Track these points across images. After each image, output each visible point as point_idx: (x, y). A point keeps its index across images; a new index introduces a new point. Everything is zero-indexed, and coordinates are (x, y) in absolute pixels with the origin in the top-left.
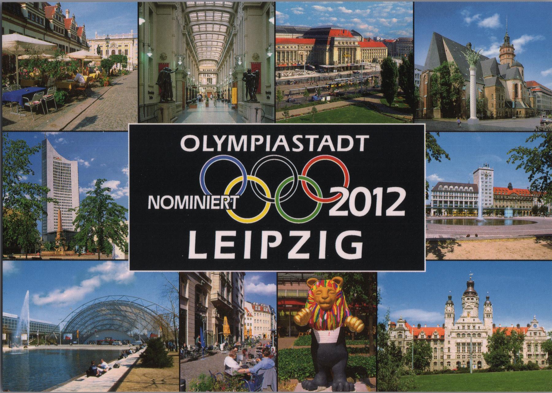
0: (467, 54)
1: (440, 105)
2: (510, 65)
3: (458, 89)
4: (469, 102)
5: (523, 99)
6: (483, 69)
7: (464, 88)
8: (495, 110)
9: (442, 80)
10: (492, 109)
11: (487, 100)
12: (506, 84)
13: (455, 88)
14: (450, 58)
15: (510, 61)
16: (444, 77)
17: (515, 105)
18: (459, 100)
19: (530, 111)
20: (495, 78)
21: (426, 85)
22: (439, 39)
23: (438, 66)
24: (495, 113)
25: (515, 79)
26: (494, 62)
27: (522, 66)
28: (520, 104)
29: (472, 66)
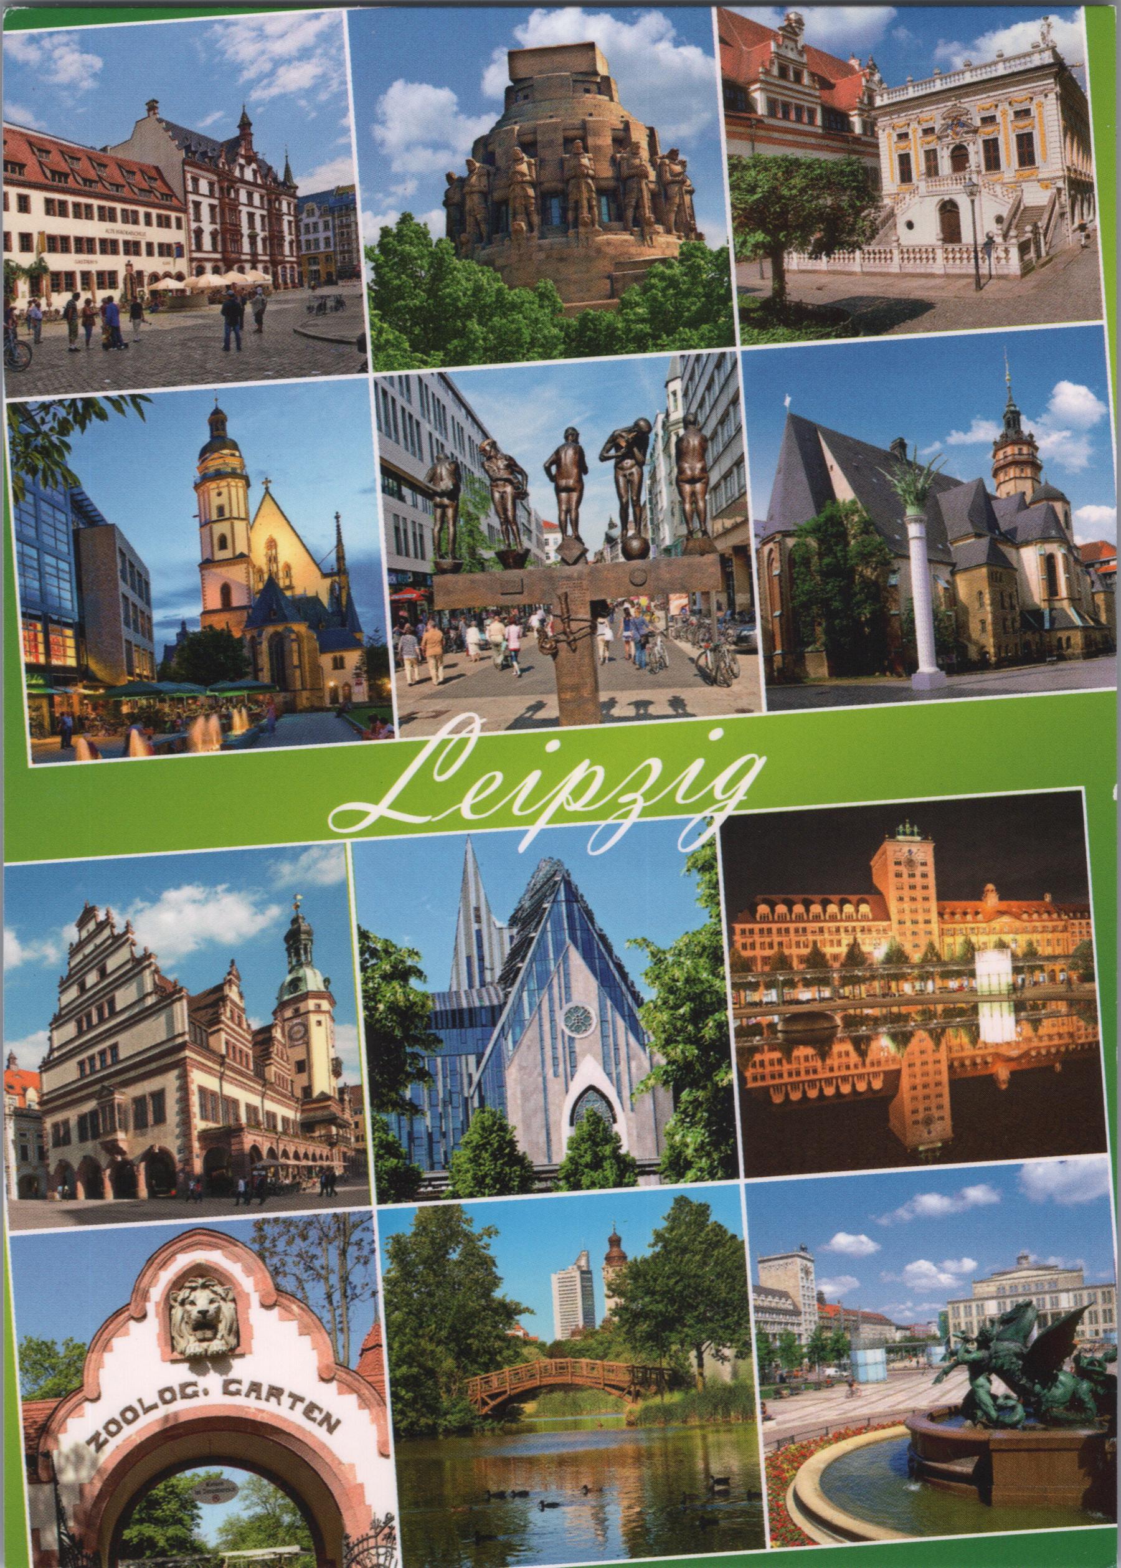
0: (893, 474)
1: (823, 638)
2: (1028, 499)
3: (875, 583)
4: (912, 621)
5: (1074, 600)
6: (946, 518)
7: (893, 580)
8: (991, 640)
9: (827, 560)
10: (983, 632)
11: (965, 610)
12: (1019, 559)
13: (865, 581)
14: (843, 490)
15: (1027, 486)
16: (830, 551)
17: (1052, 621)
18: (881, 618)
19: (1097, 636)
20: (985, 542)
21: (776, 581)
22: (805, 437)
23: (807, 515)
24: (992, 650)
25: (1045, 539)
26: (977, 493)
27: (1061, 498)
28: (1067, 616)
29: (911, 511)
